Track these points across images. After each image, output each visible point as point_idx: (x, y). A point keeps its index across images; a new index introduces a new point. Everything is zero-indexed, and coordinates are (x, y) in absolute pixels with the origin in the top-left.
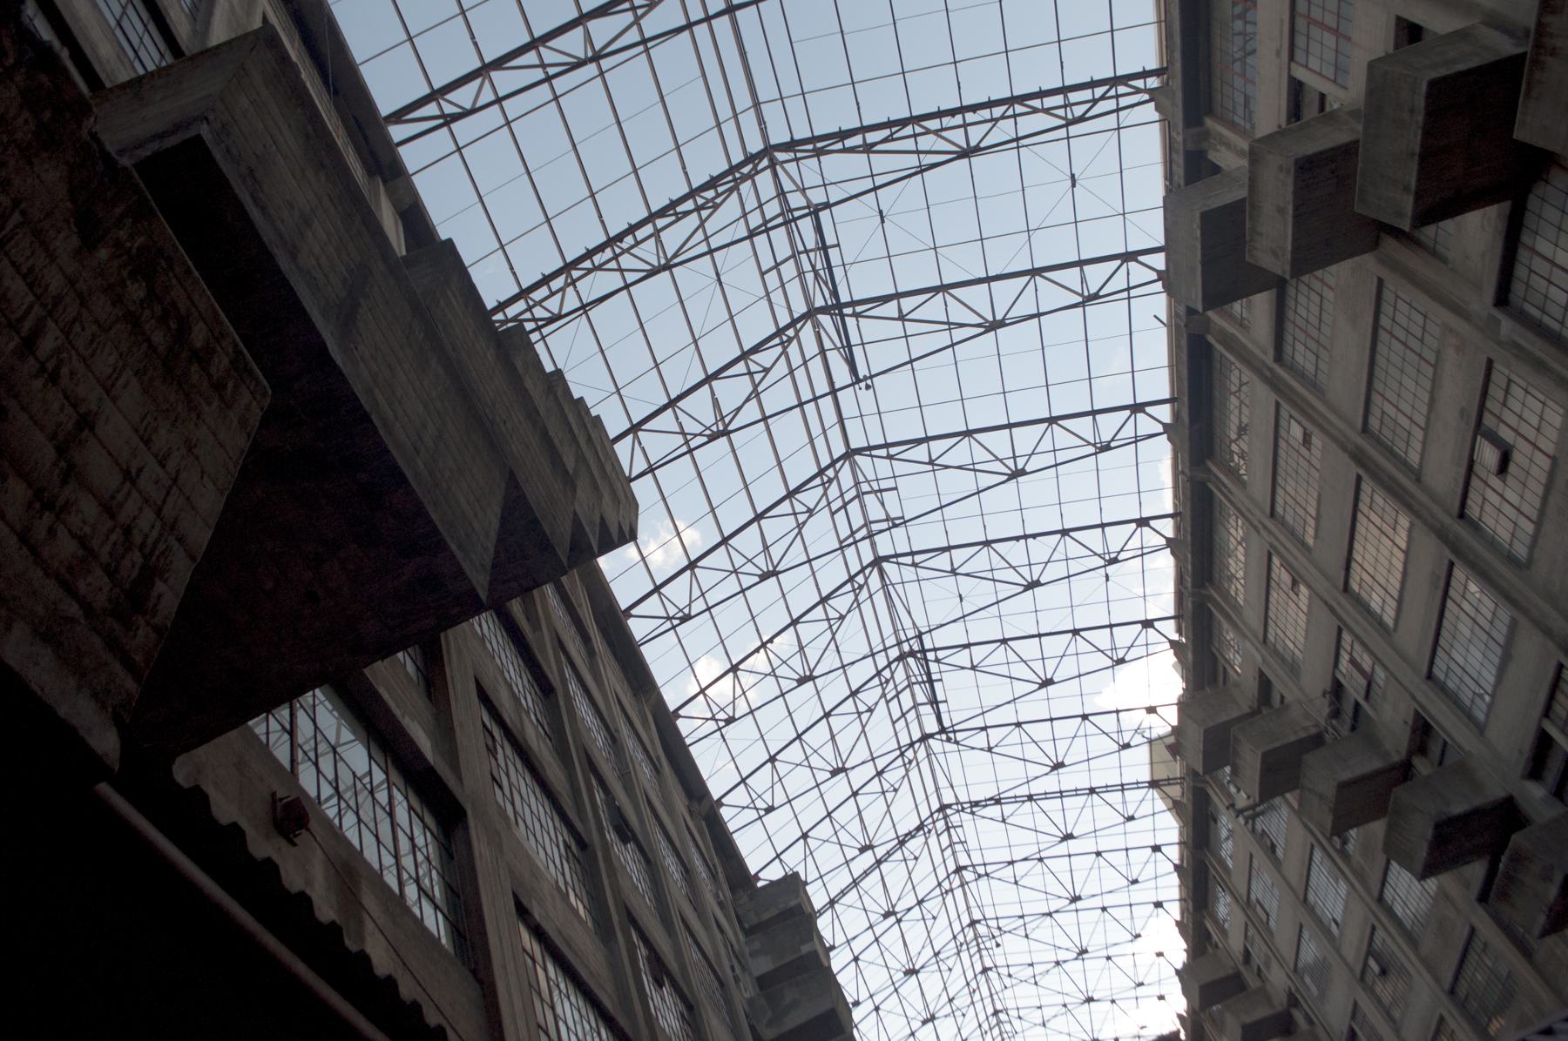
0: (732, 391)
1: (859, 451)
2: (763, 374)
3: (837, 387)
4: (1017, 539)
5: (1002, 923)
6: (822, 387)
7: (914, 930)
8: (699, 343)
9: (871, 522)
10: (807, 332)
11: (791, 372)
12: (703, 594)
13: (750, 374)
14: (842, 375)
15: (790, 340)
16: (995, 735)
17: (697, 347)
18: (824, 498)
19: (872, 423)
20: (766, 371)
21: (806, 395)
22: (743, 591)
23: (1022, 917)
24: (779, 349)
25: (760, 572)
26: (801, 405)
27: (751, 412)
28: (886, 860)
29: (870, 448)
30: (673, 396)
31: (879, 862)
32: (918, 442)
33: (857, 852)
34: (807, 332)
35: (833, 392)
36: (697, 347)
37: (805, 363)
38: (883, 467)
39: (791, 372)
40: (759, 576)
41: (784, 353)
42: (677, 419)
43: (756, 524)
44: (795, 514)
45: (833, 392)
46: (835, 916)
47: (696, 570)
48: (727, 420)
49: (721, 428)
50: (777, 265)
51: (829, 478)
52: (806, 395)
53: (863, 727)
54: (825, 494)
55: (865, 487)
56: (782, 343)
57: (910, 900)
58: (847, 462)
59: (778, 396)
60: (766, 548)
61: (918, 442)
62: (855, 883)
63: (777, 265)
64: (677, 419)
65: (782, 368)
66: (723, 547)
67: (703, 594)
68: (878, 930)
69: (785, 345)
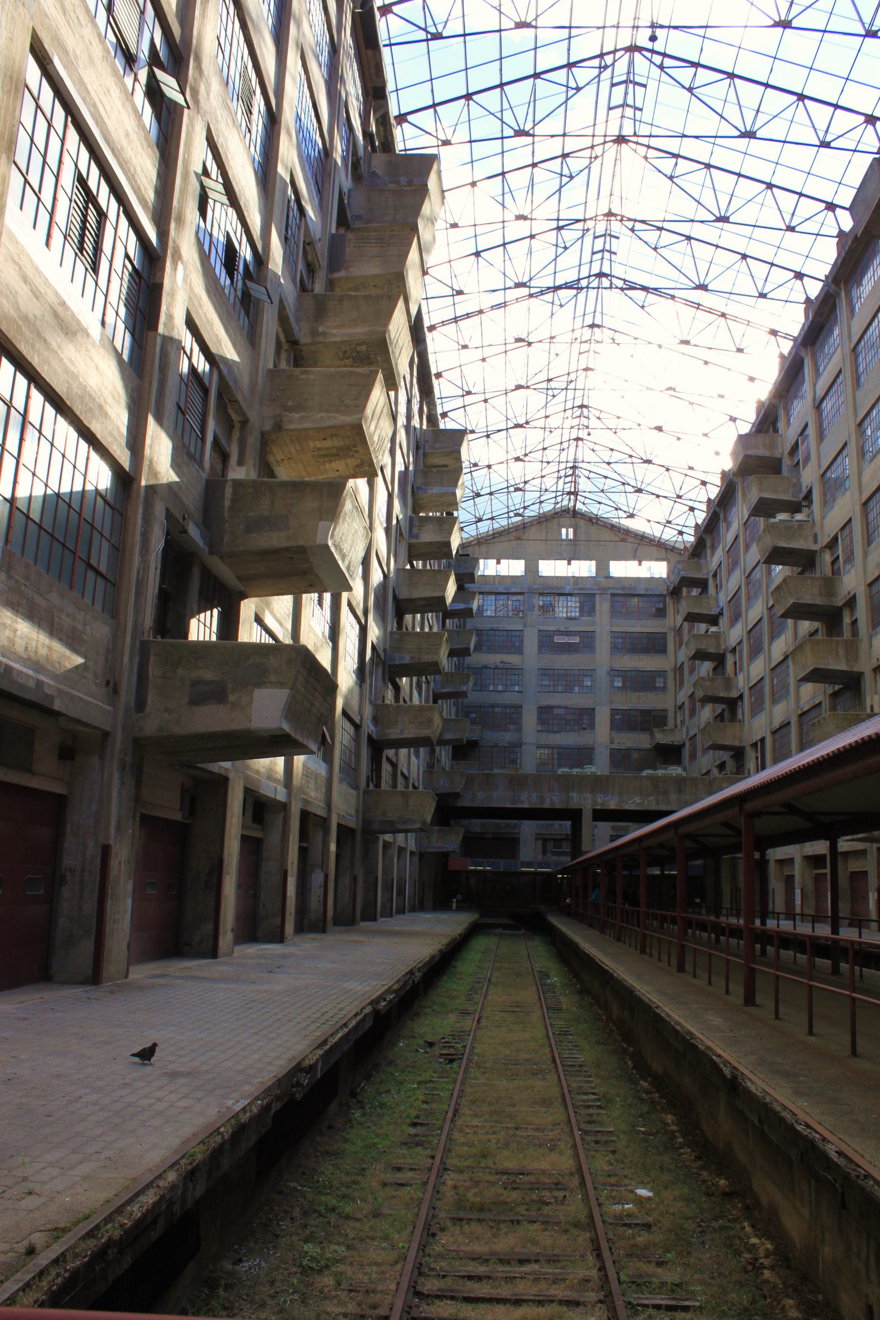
28: (536, 297)
33: (512, 285)
68: (509, 347)
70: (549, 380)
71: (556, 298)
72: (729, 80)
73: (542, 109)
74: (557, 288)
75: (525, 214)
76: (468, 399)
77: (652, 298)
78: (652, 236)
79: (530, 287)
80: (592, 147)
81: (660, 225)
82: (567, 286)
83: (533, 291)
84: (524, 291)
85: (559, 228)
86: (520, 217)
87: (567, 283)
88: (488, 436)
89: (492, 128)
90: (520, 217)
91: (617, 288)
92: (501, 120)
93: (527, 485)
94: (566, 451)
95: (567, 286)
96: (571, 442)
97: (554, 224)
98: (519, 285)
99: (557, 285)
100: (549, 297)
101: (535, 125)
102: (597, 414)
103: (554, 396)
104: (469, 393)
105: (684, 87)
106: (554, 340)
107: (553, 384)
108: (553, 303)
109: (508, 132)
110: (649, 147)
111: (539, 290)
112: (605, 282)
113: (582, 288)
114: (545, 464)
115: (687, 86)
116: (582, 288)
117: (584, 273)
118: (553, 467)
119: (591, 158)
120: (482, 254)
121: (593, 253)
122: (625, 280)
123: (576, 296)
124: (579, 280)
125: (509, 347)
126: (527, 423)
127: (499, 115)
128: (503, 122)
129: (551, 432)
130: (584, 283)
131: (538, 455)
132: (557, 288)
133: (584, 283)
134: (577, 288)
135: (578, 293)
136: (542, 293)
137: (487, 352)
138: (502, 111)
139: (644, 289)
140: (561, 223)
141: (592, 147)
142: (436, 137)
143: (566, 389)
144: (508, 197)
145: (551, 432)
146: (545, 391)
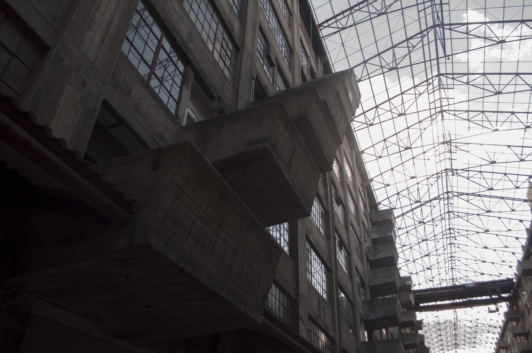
0: (400, 52)
1: (442, 75)
2: (413, 48)
3: (439, 57)
4: (494, 112)
5: (460, 231)
6: (434, 56)
7: (429, 228)
8: (392, 35)
9: (442, 98)
10: (431, 34)
11: (423, 46)
12: (379, 116)
13: (408, 47)
14: (441, 54)
15: (425, 36)
16: (471, 174)
17: (391, 36)
18: (427, 89)
19: (449, 66)
20: (414, 47)
21: (427, 58)
22: (393, 118)
23: (467, 231)
24: (420, 39)
25: (399, 113)
26: (425, 62)
27: (406, 62)
28: (423, 205)
29: (447, 74)
30: (380, 52)
31: (421, 205)
32: (465, 74)
34: (431, 34)
35: (438, 59)
36: (391, 36)
37: (429, 43)
38: (450, 81)
39: (423, 46)
40: (398, 114)
41: (422, 40)
42: (380, 59)
43: (401, 95)
44: (415, 94)
45: (438, 59)
46: (403, 218)
47: (378, 109)
48: (398, 62)
49: (394, 66)
50: (430, 60)
51: (430, 83)
52: (427, 58)
53: (431, 212)
54: (427, 88)
55: (442, 87)
56: (422, 37)
57: (430, 218)
58: (438, 77)
59: (417, 56)
60: (403, 103)
61: (465, 74)
62: (412, 210)
63: (430, 60)
64: (380, 59)
65: (420, 45)
66: (388, 102)
67: (379, 116)
68: (416, 226)
69: (422, 37)
70: (435, 236)
71: (432, 204)
72: (482, 113)
73: (413, 139)
74: (431, 201)
75: (414, 176)
76: (404, 248)
77: (470, 197)
78: (465, 174)
79: (420, 202)
80: (434, 147)
81: (468, 169)
82: (435, 199)
83: (422, 203)
84: (419, 204)
85: (428, 179)
86: (412, 178)
87: (435, 198)
88: (414, 261)
89: (396, 148)
90: (412, 178)
91: (456, 196)
92: (398, 145)
93: (432, 267)
94: (446, 249)
95: (435, 199)
96: (450, 270)
97: (426, 177)
98: (416, 202)
99: (431, 199)
100: (429, 204)
101: (411, 145)
102: (458, 259)
103: (438, 242)
104: (404, 246)
105: (465, 120)
106: (434, 220)
107: (437, 237)
108: (431, 206)
109: (402, 149)
110: (456, 143)
111: (424, 202)
112: (450, 195)
113: (441, 199)
114: (440, 269)
115: (466, 119)
116: (441, 199)
117: (441, 193)
118: (443, 270)
119: (437, 177)
120: (400, 193)
121: (444, 205)
122: (458, 192)
123: (439, 202)
124: (439, 196)
125: (416, 226)
126: (429, 254)
127: (397, 144)
128: (399, 146)
129: (440, 256)
130: (442, 197)
131: (435, 253)
132: (431, 201)
133: (442, 197)
134: (439, 199)
135: (440, 201)
136: (425, 203)
137: (408, 229)
138: (398, 142)
139: (467, 194)
140: (428, 177)
141: (434, 147)
142: (376, 156)
143: (443, 238)
144: (405, 170)
145: (440, 256)
146: (434, 240)
